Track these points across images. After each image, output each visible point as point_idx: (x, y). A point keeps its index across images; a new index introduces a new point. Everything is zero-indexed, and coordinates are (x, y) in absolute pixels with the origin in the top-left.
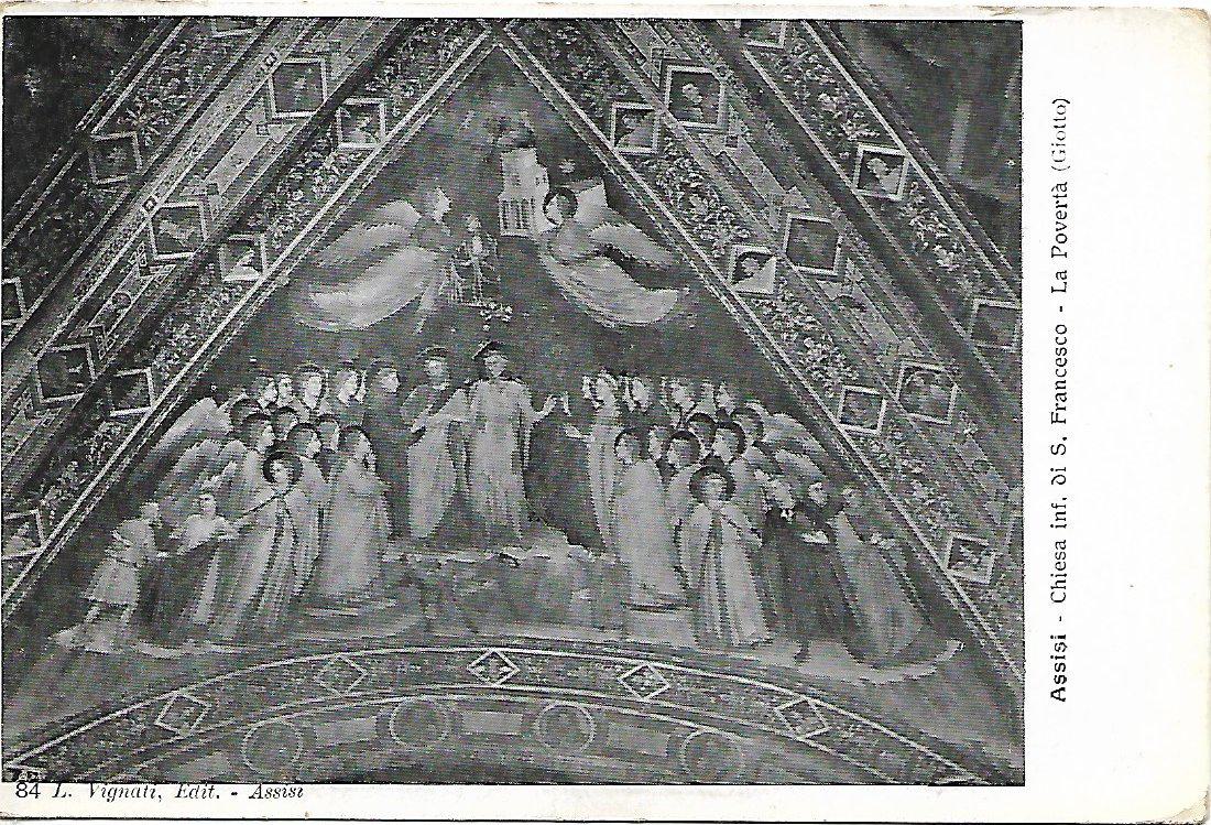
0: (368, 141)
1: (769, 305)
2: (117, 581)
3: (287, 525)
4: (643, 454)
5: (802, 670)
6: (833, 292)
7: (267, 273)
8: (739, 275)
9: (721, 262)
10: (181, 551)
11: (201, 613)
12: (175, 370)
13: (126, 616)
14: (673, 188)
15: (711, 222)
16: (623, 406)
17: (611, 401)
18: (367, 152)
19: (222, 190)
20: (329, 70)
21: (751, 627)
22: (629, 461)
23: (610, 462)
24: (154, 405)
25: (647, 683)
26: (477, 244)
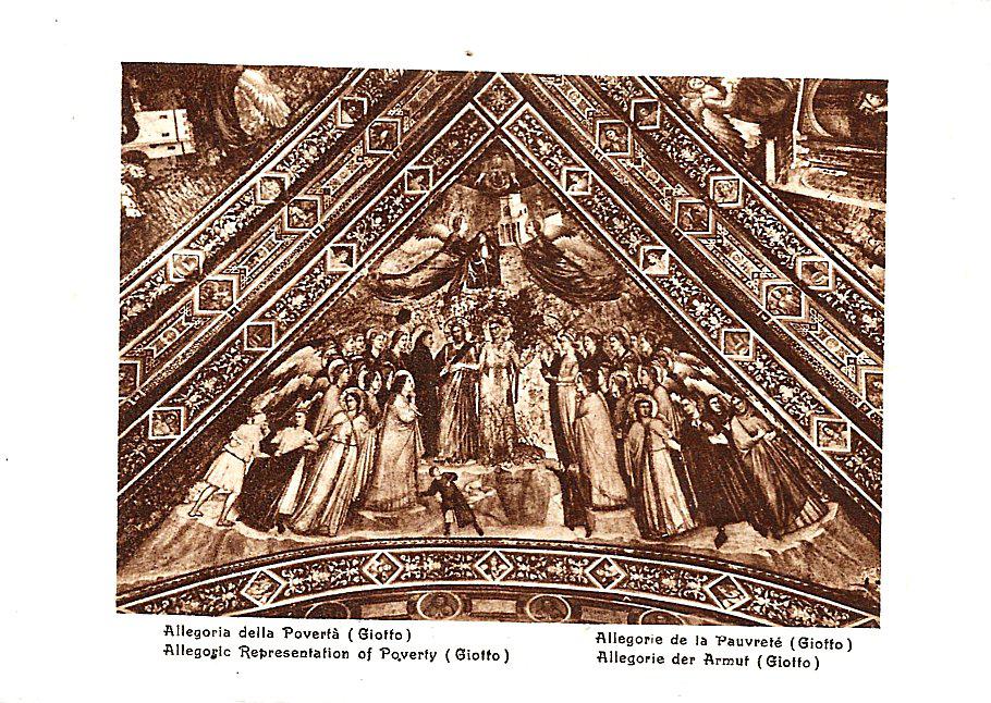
0: (422, 189)
1: (667, 282)
2: (229, 472)
3: (353, 443)
4: (594, 388)
5: (722, 550)
6: (712, 244)
7: (355, 266)
8: (647, 264)
9: (635, 256)
10: (277, 454)
11: (286, 505)
12: (290, 325)
13: (232, 499)
14: (602, 214)
15: (628, 232)
16: (577, 354)
17: (571, 351)
18: (421, 196)
19: (332, 193)
20: (402, 127)
21: (679, 516)
22: (585, 393)
23: (572, 394)
24: (274, 346)
25: (607, 574)
26: (485, 249)
